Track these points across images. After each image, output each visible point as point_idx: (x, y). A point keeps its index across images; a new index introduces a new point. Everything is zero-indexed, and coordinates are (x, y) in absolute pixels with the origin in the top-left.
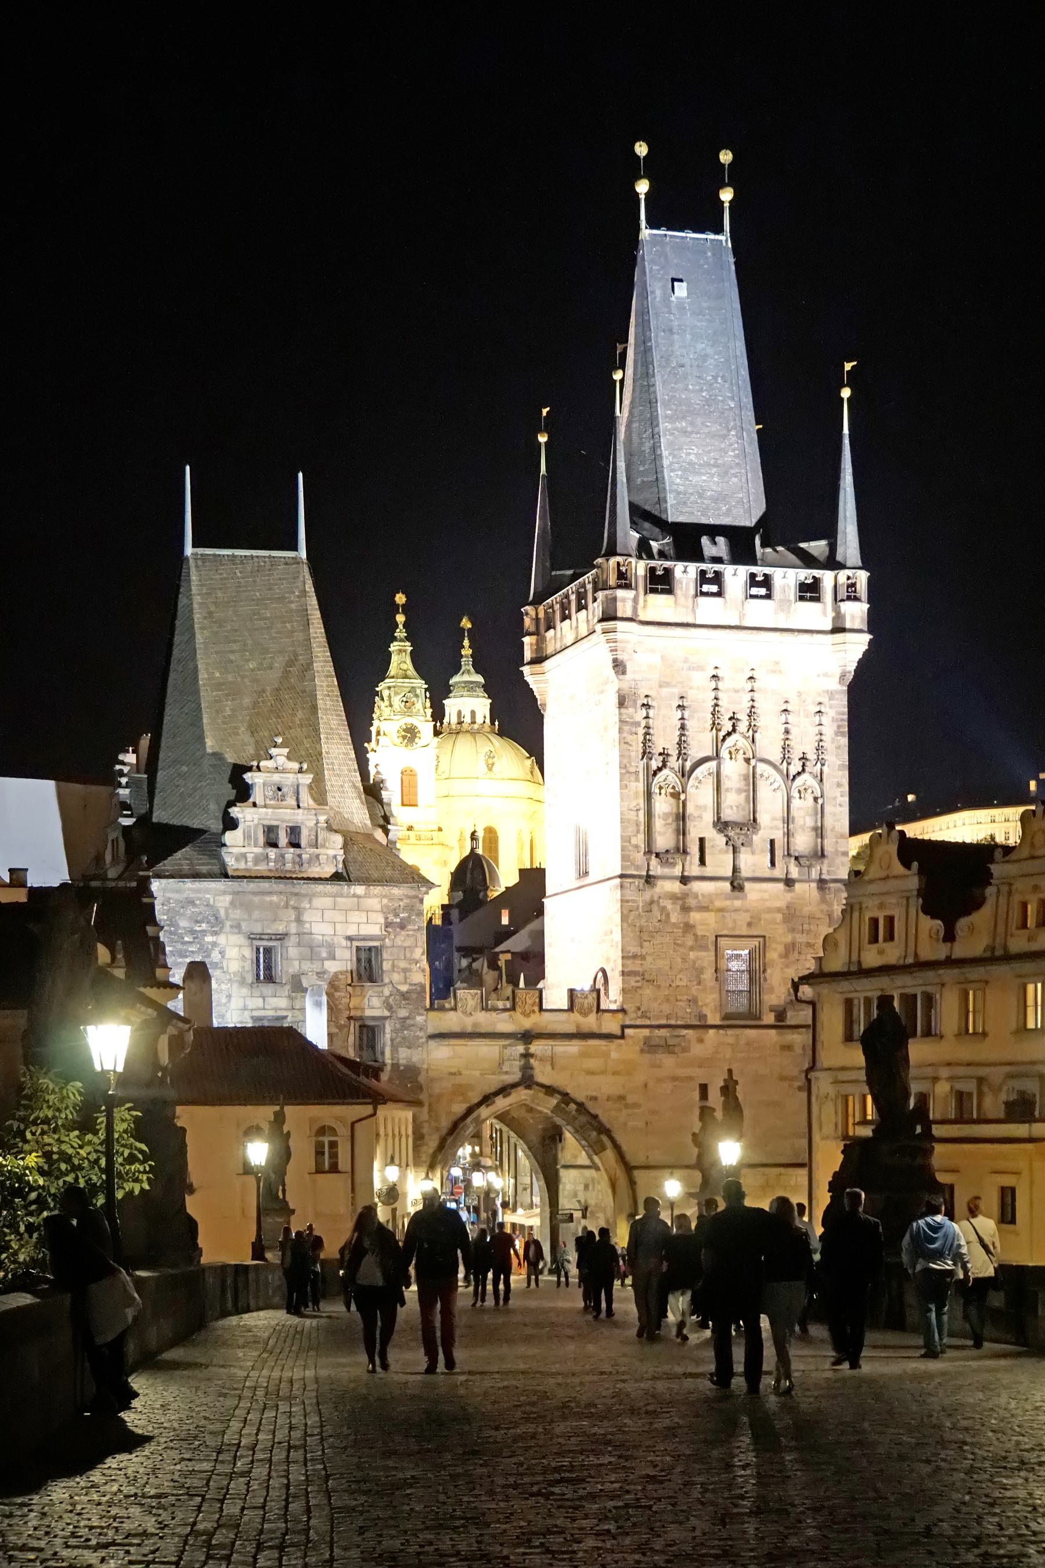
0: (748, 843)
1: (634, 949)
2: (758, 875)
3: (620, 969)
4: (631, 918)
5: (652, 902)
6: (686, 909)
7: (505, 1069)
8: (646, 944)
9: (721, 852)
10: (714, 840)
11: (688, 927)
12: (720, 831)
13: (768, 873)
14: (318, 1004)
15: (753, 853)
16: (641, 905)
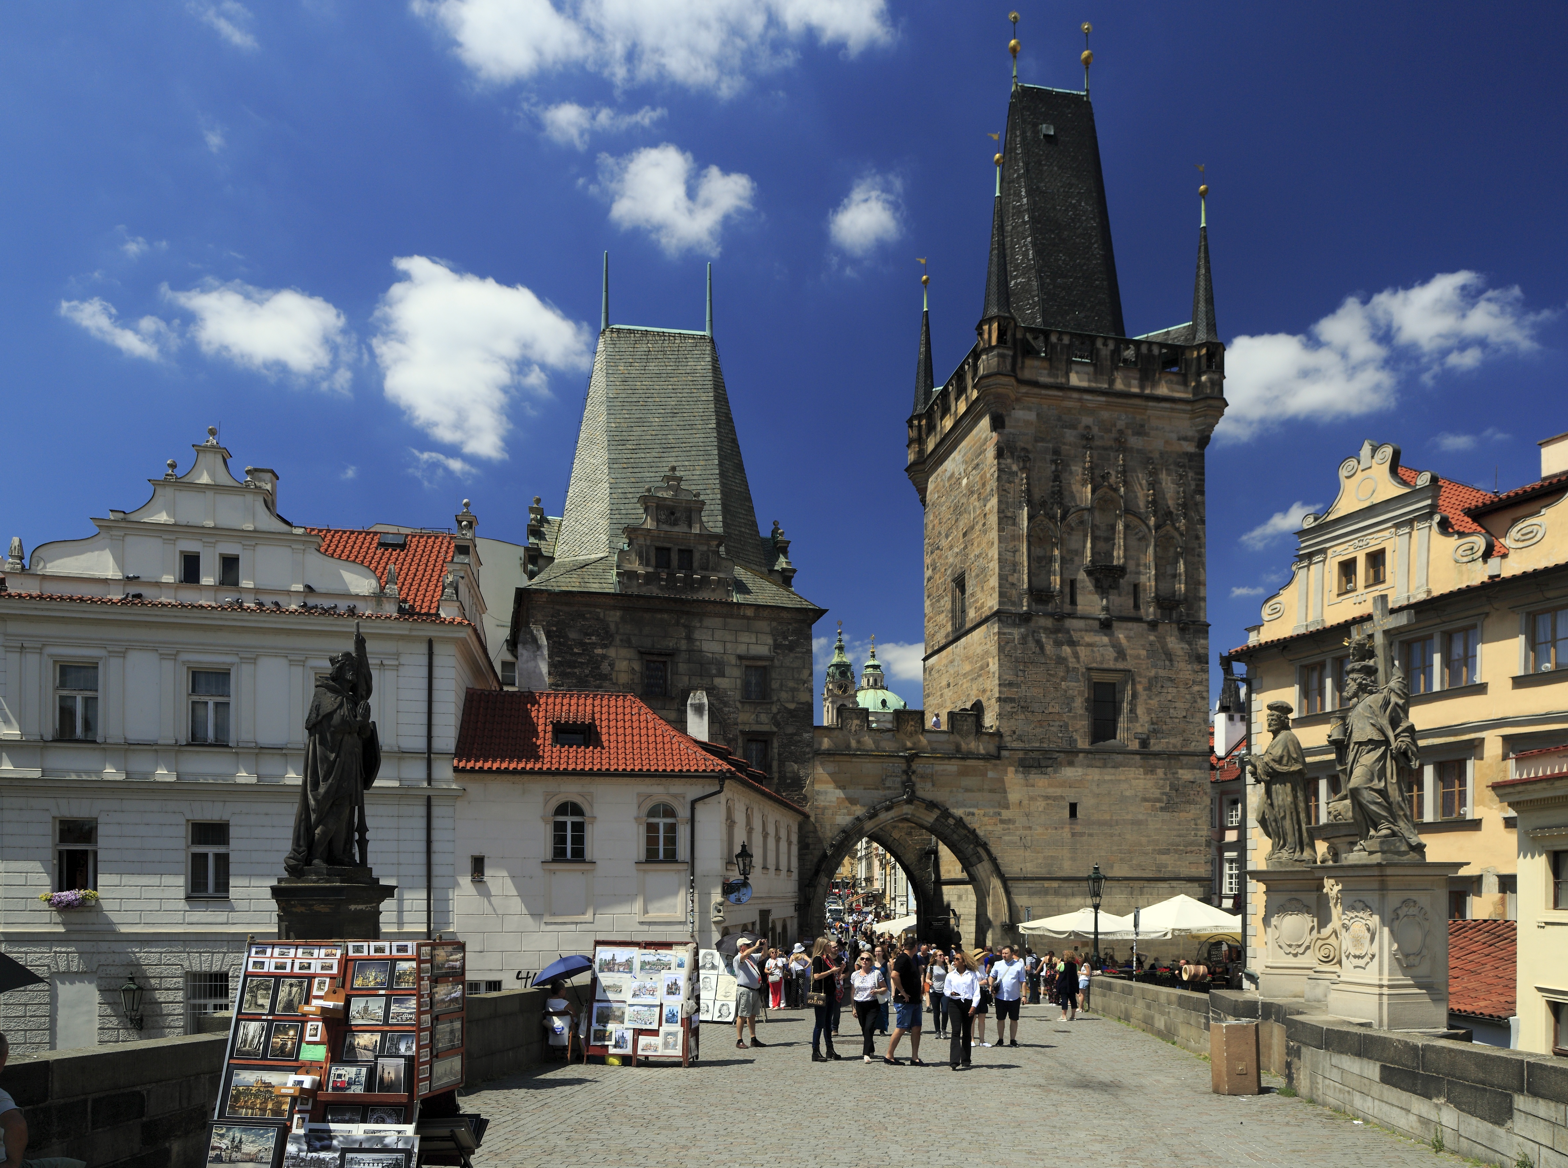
0: (1115, 586)
1: (1009, 677)
2: (1124, 614)
3: (997, 695)
4: (1007, 649)
5: (1027, 635)
6: (1058, 644)
7: (888, 784)
8: (1020, 673)
9: (1090, 593)
10: (1083, 581)
11: (1061, 660)
12: (1089, 573)
13: (1132, 613)
14: (699, 709)
15: (1120, 595)
16: (1017, 637)
